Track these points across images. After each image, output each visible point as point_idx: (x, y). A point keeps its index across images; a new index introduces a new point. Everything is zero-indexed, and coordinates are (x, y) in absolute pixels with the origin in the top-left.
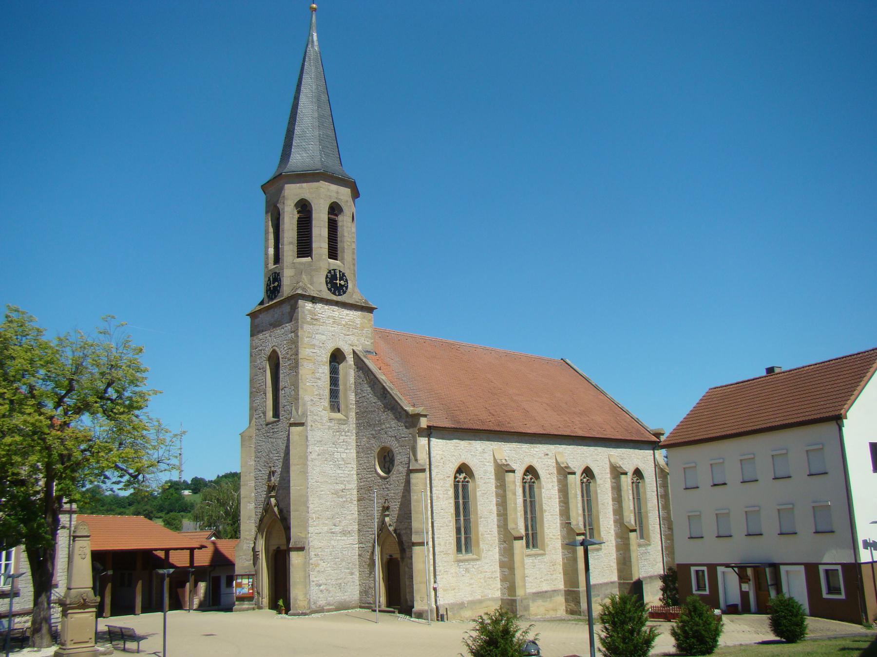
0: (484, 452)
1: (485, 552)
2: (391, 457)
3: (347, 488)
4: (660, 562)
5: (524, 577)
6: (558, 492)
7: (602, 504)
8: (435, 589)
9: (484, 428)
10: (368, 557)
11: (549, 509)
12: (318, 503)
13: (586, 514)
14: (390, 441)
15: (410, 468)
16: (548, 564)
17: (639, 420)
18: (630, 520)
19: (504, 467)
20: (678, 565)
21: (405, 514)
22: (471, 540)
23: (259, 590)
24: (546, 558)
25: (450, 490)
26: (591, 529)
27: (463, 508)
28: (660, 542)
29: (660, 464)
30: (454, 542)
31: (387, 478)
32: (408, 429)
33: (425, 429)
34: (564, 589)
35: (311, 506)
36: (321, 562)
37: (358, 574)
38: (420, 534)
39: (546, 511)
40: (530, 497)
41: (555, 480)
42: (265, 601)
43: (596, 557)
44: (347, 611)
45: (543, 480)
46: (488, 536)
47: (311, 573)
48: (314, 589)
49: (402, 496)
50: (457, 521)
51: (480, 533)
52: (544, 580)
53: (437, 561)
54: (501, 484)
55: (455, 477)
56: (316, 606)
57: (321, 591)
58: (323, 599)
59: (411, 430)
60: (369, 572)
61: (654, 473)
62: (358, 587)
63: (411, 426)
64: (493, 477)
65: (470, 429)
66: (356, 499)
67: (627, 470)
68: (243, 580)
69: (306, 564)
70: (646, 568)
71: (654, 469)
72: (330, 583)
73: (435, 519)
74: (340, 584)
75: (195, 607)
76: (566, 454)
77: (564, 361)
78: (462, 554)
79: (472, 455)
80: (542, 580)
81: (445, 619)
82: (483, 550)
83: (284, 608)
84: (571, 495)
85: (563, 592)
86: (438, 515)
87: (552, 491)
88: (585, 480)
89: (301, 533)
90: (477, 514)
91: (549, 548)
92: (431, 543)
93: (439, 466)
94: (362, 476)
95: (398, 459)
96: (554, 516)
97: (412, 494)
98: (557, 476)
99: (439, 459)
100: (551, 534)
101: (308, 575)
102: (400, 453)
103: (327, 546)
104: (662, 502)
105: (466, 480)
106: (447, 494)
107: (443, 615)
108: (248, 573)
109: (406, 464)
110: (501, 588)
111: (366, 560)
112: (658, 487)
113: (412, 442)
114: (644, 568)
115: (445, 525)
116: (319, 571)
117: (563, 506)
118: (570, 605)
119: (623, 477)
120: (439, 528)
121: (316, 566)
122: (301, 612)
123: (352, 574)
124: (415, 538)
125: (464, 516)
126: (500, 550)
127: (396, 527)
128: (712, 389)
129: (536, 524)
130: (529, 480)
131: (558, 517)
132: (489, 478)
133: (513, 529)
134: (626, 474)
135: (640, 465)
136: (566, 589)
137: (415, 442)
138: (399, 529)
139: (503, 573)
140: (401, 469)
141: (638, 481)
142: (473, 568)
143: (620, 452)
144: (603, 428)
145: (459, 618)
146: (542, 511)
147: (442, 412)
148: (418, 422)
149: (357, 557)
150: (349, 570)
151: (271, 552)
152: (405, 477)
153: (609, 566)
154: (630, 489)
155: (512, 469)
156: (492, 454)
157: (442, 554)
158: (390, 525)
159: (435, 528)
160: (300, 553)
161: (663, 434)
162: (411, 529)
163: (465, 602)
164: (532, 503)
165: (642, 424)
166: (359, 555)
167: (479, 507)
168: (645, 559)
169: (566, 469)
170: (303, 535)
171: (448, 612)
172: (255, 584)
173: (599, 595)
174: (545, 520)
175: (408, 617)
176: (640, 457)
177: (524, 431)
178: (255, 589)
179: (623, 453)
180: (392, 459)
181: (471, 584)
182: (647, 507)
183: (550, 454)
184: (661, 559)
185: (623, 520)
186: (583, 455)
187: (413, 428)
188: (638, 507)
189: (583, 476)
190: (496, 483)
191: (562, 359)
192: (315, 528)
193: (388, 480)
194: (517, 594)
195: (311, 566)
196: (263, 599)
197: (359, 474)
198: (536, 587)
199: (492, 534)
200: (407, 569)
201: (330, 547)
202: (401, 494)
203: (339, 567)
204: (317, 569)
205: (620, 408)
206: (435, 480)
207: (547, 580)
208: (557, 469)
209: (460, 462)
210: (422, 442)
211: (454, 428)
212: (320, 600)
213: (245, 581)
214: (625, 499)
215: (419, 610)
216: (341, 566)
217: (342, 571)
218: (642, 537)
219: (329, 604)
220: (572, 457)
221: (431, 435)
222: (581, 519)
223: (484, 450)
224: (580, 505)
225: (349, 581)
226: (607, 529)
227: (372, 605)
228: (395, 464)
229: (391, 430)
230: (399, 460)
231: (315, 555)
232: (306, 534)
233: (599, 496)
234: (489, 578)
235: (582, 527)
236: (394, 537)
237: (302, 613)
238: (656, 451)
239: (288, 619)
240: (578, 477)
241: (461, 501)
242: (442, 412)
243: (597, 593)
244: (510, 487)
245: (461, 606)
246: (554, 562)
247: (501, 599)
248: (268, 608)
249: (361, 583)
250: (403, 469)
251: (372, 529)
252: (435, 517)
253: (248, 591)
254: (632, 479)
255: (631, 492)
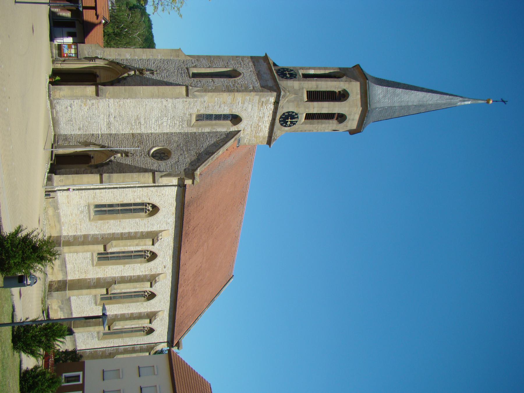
0: (167, 223)
1: (96, 224)
2: (164, 158)
3: (142, 126)
4: (86, 347)
5: (77, 252)
6: (138, 275)
7: (129, 306)
8: (69, 189)
9: (184, 224)
10: (92, 141)
11: (126, 269)
12: (131, 105)
13: (122, 295)
14: (175, 157)
15: (156, 173)
16: (86, 268)
17: (189, 331)
18: (117, 326)
19: (156, 237)
20: (84, 363)
21: (123, 169)
22: (104, 214)
23: (67, 62)
24: (90, 267)
25: (140, 199)
26: (111, 298)
27: (127, 209)
28: (100, 347)
29: (157, 346)
30: (103, 203)
31: (148, 155)
32: (184, 171)
33: (184, 183)
34: (68, 279)
35: (128, 101)
36: (88, 107)
37: (79, 133)
38: (108, 179)
39: (124, 266)
40: (134, 256)
41: (147, 273)
42: (59, 66)
43: (90, 302)
44: (52, 125)
45: (147, 264)
46: (107, 227)
47: (80, 101)
48: (67, 102)
49: (136, 166)
50: (118, 205)
51: (109, 221)
52: (75, 266)
53: (88, 191)
54: (144, 236)
55: (149, 204)
56: (56, 104)
57: (67, 108)
58: (60, 108)
59: (183, 173)
60: (81, 141)
61: (151, 342)
62: (70, 133)
63: (186, 173)
64: (149, 230)
65: (183, 214)
66: (134, 132)
67: (153, 323)
68: (74, 49)
69: (86, 97)
70: (82, 337)
71: (153, 342)
72: (73, 114)
73: (119, 189)
74: (72, 121)
75: (53, 9)
76: (165, 281)
77: (232, 277)
78: (94, 208)
79: (165, 215)
80: (75, 264)
81: (47, 197)
82: (97, 223)
83: (54, 80)
84: (136, 284)
85: (65, 279)
86: (122, 192)
87: (139, 271)
88: (146, 294)
89: (109, 94)
90: (123, 219)
91: (97, 269)
92: (102, 187)
93: (158, 192)
94: (150, 137)
95: (163, 163)
96: (120, 272)
97: (137, 173)
98: (149, 274)
99: (162, 192)
100: (108, 270)
101: (78, 98)
102: (167, 165)
103: (99, 112)
104: (129, 348)
105: (147, 211)
106: (137, 198)
107: (50, 196)
108: (79, 53)
109: (159, 169)
110: (69, 235)
111: (89, 139)
112: (140, 345)
113: (175, 173)
114: (82, 336)
115: (115, 197)
116: (81, 106)
117: (128, 279)
118: (56, 284)
119: (148, 321)
120: (113, 193)
121: (85, 104)
122: (51, 93)
123: (79, 129)
124: (105, 176)
125: (121, 209)
126: (97, 234)
127: (113, 162)
128: (210, 385)
129: (115, 260)
130: (147, 255)
131: (120, 275)
132: (148, 227)
133: (112, 244)
134: (150, 322)
135: (156, 332)
136: (68, 281)
137: (175, 176)
138: (112, 164)
139: (80, 238)
140: (155, 165)
141: (145, 331)
142: (84, 216)
143: (166, 318)
144: (183, 306)
145: (47, 206)
146: (125, 264)
147: (196, 194)
148: (188, 178)
149: (92, 133)
150: (82, 127)
151: (95, 71)
152: (149, 168)
153: (84, 311)
154: (139, 326)
155: (154, 244)
156: (165, 229)
157: (94, 194)
158: (115, 157)
159: (113, 190)
160: (94, 93)
161: (178, 349)
162: (112, 173)
163: (59, 211)
164: (130, 257)
165: (186, 334)
166: (93, 135)
167: (127, 220)
168: (88, 336)
169: (154, 280)
170: (107, 95)
171: (52, 199)
172: (71, 59)
173: (62, 304)
174: (118, 266)
175: (48, 171)
176: (162, 332)
177: (182, 251)
178: (67, 59)
179: (165, 320)
180: (162, 158)
181: (72, 215)
182: (126, 337)
183: (165, 270)
184: (88, 348)
185: (117, 321)
186: (164, 292)
187: (185, 174)
188: (125, 331)
189: (149, 292)
190: (144, 232)
191: (233, 276)
192: (113, 103)
193: (147, 156)
194: (64, 247)
195: (85, 100)
196: (60, 64)
197: (151, 134)
198: (69, 260)
199: (108, 229)
200: (83, 169)
201: (99, 114)
202: (137, 165)
203: (84, 120)
204: (83, 105)
205: (198, 318)
206: (147, 189)
207: (74, 268)
208: (154, 274)
209: (160, 207)
210: (175, 181)
211: (184, 203)
212: (60, 106)
213: (73, 51)
214: (132, 322)
215: (53, 179)
216: (85, 121)
217: (82, 122)
218: (105, 334)
219: (57, 113)
220: (163, 285)
221: (179, 187)
222: (118, 291)
223: (169, 223)
224: (128, 290)
225: (74, 127)
226: (111, 309)
227: (56, 144)
228: (159, 161)
229: (183, 158)
230: (162, 164)
231: (93, 103)
232: (107, 97)
233: (135, 304)
234: (76, 227)
235: (113, 292)
236: (106, 160)
237: (50, 94)
238: (166, 343)
239: (46, 85)
240: (149, 289)
241: (132, 207)
242: (196, 194)
243: (64, 303)
244: (142, 241)
245: (56, 208)
246: (88, 272)
247: (61, 236)
248: (54, 67)
249: (72, 135)
250: (155, 167)
251: (112, 144)
252: (120, 189)
253: (66, 54)
254: (146, 327)
255: (137, 326)
